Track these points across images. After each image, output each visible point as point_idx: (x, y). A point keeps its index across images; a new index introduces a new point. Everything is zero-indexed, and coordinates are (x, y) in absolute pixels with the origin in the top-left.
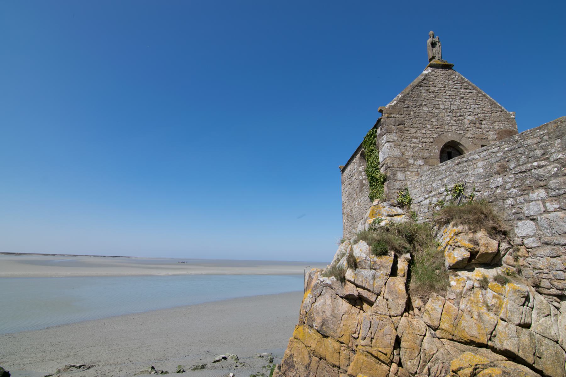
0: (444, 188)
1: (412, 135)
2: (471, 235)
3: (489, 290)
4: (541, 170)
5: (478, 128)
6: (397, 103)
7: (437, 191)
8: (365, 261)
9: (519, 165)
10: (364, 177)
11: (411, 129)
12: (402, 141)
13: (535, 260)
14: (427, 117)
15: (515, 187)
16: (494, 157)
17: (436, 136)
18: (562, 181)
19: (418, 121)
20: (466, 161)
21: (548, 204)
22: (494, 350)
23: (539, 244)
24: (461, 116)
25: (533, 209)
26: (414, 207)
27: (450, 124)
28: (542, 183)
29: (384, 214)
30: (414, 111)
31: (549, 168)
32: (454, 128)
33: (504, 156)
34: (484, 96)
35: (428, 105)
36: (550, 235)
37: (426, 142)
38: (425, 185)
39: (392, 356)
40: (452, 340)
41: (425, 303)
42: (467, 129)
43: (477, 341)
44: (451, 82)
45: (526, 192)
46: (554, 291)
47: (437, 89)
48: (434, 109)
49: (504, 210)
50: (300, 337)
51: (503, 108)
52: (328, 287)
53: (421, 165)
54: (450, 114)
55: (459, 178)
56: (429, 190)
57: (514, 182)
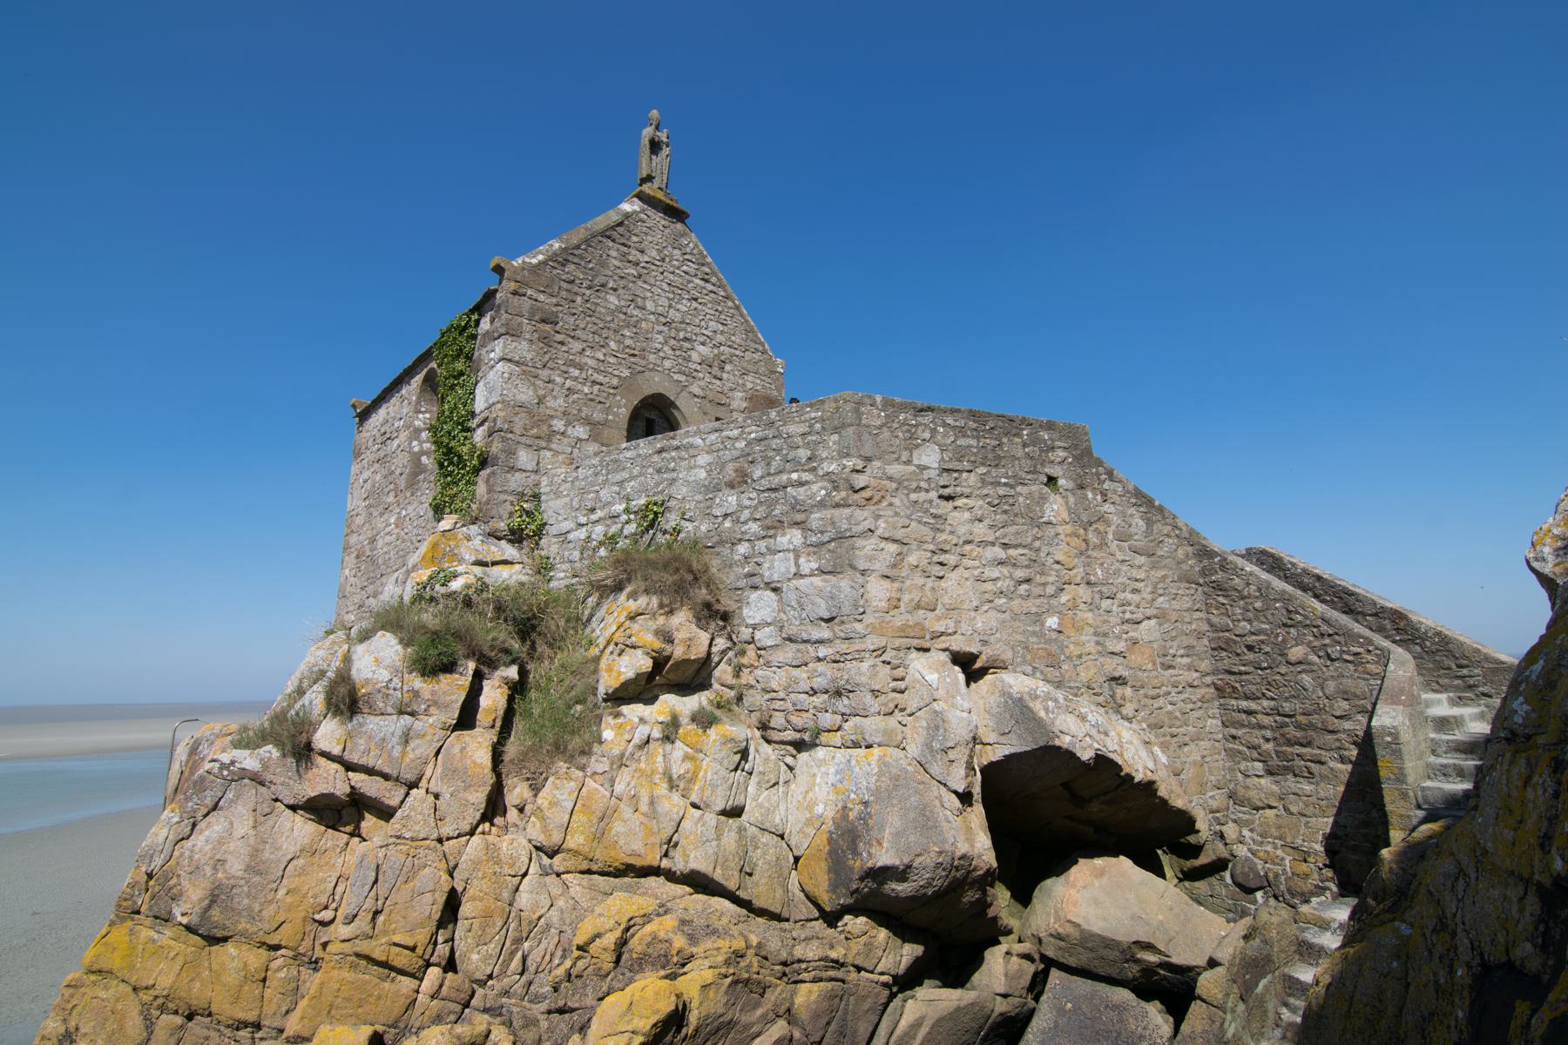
0: (624, 505)
1: (571, 357)
2: (661, 620)
3: (678, 744)
4: (801, 490)
5: (715, 377)
6: (544, 263)
7: (606, 510)
8: (384, 690)
9: (769, 474)
10: (427, 446)
11: (570, 340)
12: (544, 366)
13: (768, 673)
14: (613, 320)
15: (756, 519)
16: (730, 450)
17: (626, 373)
18: (829, 516)
19: (590, 325)
20: (677, 448)
21: (802, 560)
22: (671, 876)
23: (778, 640)
24: (686, 339)
25: (776, 568)
26: (549, 546)
27: (661, 354)
28: (799, 517)
29: (467, 557)
30: (586, 298)
31: (815, 488)
32: (667, 364)
33: (747, 450)
34: (737, 308)
35: (621, 291)
36: (797, 623)
37: (602, 384)
38: (583, 492)
39: (431, 947)
40: (589, 872)
41: (536, 789)
42: (695, 374)
43: (638, 862)
44: (677, 252)
45: (771, 532)
46: (790, 735)
47: (647, 259)
48: (632, 307)
49: (731, 566)
50: (115, 962)
51: (767, 346)
52: (246, 781)
53: (581, 440)
54: (665, 329)
55: (657, 485)
57: (756, 508)
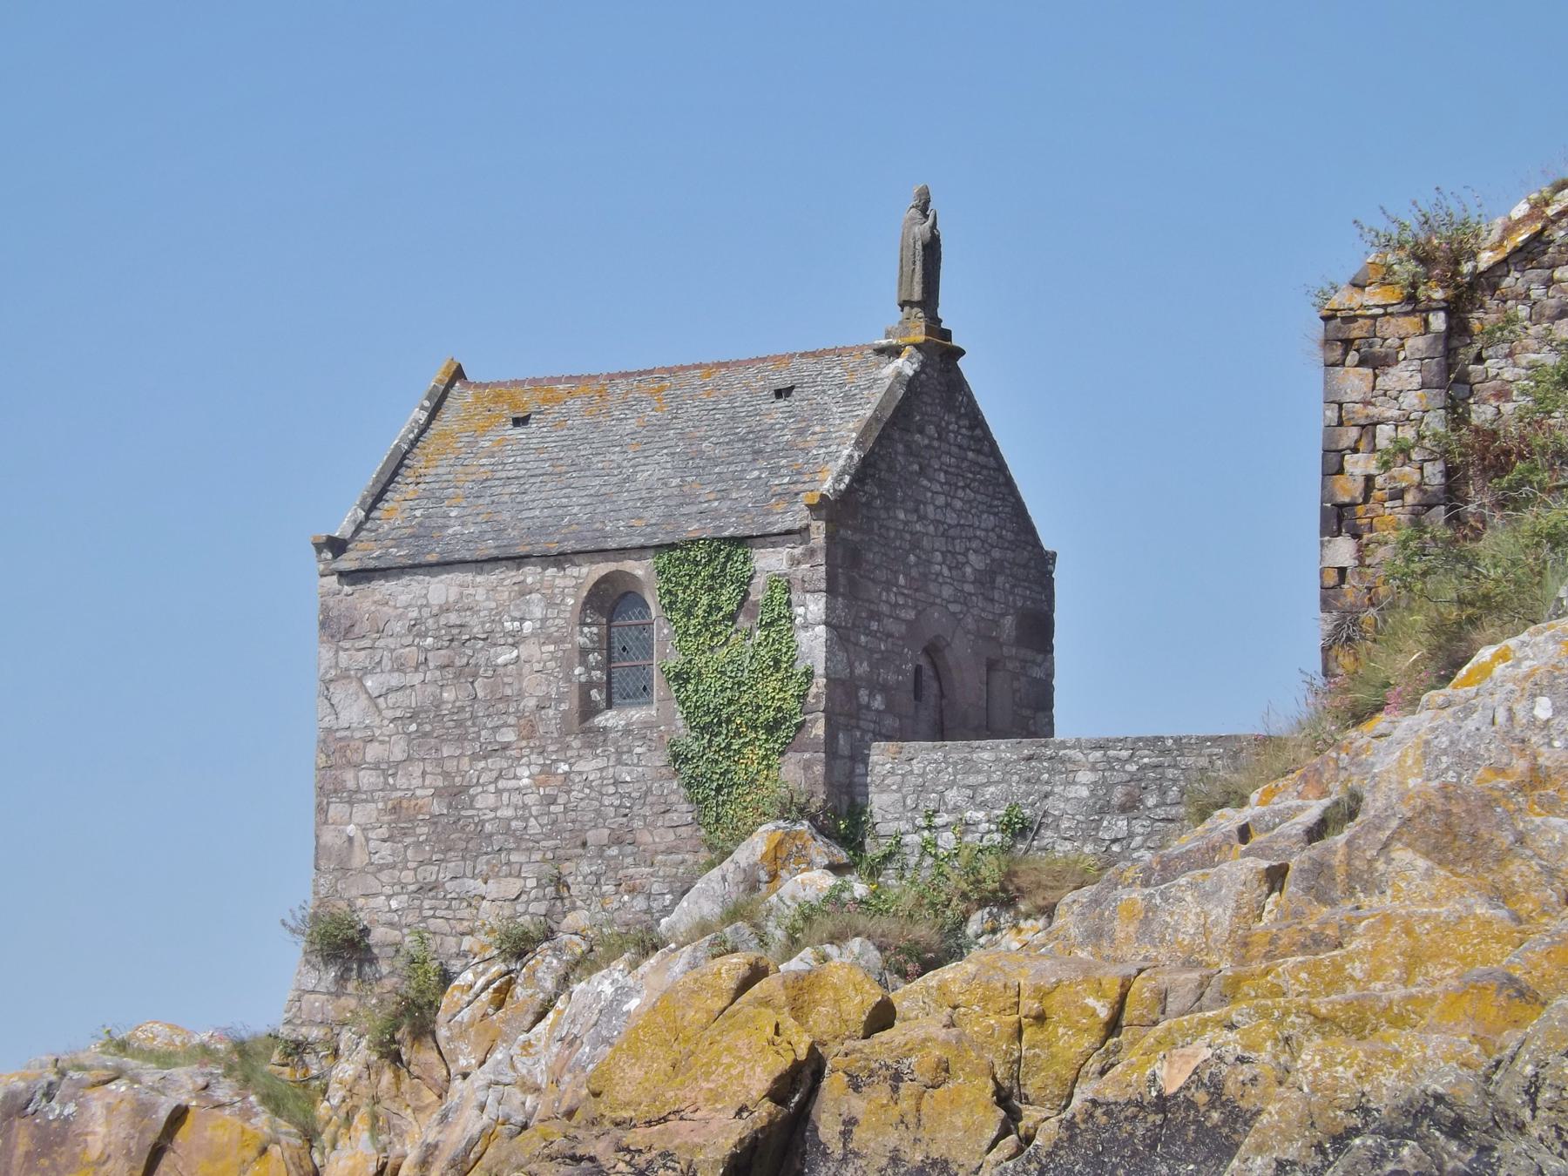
10: (597, 674)
15: (1149, 848)
29: (818, 860)
33: (1139, 775)
38: (921, 789)
56: (932, 806)
